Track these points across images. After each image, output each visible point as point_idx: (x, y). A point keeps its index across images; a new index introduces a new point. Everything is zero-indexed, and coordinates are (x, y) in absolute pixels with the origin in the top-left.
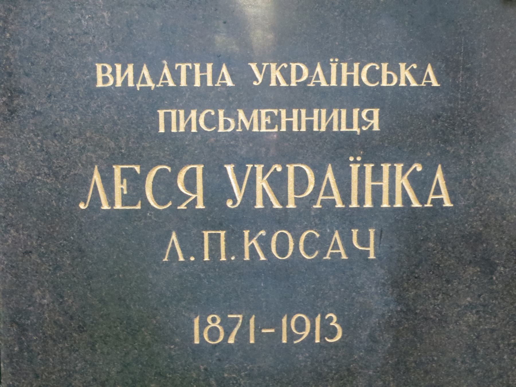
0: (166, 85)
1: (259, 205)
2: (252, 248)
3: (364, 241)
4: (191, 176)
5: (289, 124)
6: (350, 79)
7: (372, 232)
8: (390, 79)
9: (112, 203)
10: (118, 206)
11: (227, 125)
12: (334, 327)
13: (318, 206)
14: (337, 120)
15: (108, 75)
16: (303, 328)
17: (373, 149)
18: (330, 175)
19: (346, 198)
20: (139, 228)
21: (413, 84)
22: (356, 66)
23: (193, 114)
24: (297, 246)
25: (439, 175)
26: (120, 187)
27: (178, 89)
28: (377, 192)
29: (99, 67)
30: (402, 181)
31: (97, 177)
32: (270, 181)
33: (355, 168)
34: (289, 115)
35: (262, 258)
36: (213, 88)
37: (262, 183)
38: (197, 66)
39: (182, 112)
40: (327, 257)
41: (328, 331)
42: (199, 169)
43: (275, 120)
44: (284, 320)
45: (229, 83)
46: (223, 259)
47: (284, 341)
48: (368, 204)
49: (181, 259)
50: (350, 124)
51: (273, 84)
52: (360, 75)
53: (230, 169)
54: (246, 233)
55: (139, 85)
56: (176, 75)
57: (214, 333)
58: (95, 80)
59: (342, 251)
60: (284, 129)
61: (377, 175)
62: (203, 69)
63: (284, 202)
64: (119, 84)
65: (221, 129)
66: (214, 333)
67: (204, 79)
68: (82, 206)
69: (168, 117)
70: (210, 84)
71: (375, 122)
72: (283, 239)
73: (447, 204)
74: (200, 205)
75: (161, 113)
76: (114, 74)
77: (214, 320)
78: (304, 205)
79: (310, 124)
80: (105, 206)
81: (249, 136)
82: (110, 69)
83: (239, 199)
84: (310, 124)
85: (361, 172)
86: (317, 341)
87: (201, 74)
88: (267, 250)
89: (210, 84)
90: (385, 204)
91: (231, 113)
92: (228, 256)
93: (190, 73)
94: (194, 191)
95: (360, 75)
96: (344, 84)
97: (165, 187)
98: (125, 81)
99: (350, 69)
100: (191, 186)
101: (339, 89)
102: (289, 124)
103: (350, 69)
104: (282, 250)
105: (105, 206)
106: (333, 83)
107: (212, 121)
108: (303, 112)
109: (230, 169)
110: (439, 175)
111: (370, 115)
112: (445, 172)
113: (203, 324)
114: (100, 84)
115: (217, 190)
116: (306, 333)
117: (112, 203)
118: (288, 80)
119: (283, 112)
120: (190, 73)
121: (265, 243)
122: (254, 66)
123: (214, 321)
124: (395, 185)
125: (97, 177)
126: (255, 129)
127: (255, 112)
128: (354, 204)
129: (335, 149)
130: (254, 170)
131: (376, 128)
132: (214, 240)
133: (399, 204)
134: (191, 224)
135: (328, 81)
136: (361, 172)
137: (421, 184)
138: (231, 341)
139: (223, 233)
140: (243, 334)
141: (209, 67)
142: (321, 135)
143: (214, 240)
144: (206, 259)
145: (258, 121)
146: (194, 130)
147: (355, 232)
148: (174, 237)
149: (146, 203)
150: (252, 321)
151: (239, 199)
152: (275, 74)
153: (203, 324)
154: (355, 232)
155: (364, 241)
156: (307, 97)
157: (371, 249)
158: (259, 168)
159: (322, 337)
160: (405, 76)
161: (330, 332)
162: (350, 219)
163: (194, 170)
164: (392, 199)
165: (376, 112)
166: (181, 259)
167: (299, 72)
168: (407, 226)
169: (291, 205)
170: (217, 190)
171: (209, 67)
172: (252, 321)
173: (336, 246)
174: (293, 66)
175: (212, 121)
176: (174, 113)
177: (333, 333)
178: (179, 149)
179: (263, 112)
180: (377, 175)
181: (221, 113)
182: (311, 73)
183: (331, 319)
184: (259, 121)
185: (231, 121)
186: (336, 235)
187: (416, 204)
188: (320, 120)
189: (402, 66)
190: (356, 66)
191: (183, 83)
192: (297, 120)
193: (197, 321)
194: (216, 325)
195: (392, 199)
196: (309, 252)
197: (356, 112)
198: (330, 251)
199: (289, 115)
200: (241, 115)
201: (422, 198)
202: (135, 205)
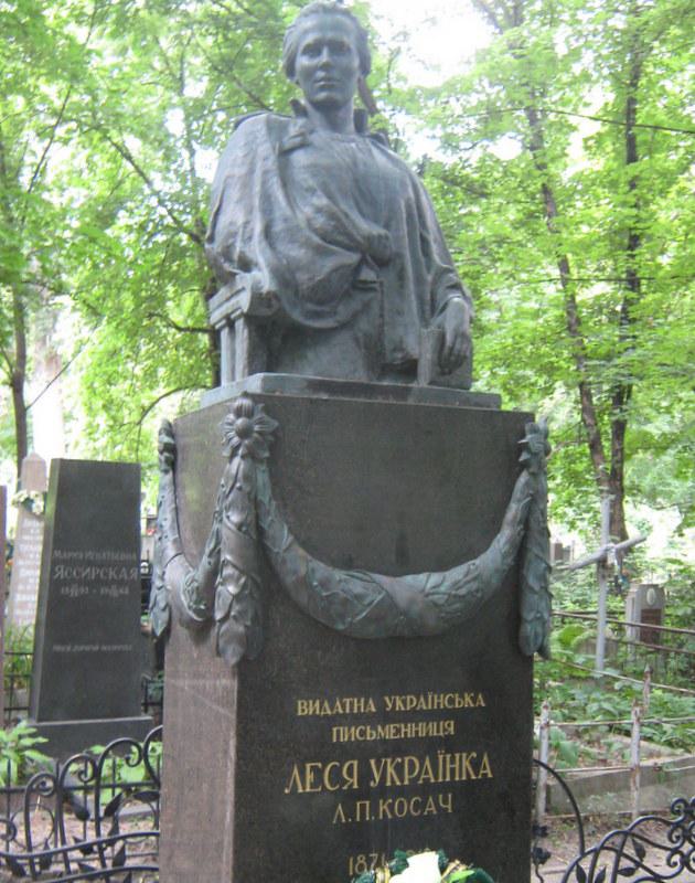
1: (389, 784)
2: (384, 811)
3: (445, 802)
4: (350, 769)
5: (406, 733)
6: (439, 704)
8: (459, 703)
9: (304, 788)
10: (308, 790)
13: (421, 782)
14: (432, 729)
15: (305, 707)
17: (450, 745)
18: (427, 763)
19: (436, 777)
21: (472, 705)
22: (442, 696)
23: (353, 729)
24: (409, 807)
25: (485, 759)
27: (344, 714)
28: (453, 770)
29: (300, 703)
30: (466, 763)
31: (296, 772)
32: (395, 768)
33: (441, 757)
34: (406, 727)
37: (390, 770)
38: (356, 701)
39: (346, 729)
40: (426, 813)
42: (355, 763)
43: (398, 731)
45: (373, 710)
46: (368, 819)
48: (448, 779)
49: (344, 821)
51: (397, 709)
52: (442, 701)
53: (373, 762)
55: (322, 713)
58: (296, 711)
59: (433, 808)
61: (453, 761)
62: (359, 702)
63: (402, 780)
64: (311, 713)
67: (359, 708)
68: (287, 791)
69: (338, 732)
70: (362, 710)
71: (452, 728)
73: (490, 776)
74: (356, 786)
75: (335, 729)
76: (308, 706)
79: (417, 732)
80: (300, 791)
81: (384, 741)
82: (305, 704)
83: (377, 780)
84: (417, 732)
87: (355, 705)
89: (362, 710)
90: (457, 779)
93: (352, 704)
95: (442, 701)
96: (435, 707)
97: (336, 776)
98: (315, 711)
99: (439, 698)
101: (432, 710)
102: (406, 733)
103: (439, 698)
104: (401, 811)
105: (300, 791)
106: (430, 707)
107: (363, 733)
109: (373, 762)
111: (449, 725)
112: (489, 756)
113: (355, 862)
114: (300, 713)
115: (365, 775)
117: (304, 788)
119: (403, 726)
120: (352, 704)
121: (391, 807)
122: (387, 699)
124: (459, 767)
128: (440, 780)
129: (428, 747)
130: (386, 763)
131: (452, 733)
132: (363, 807)
133: (464, 778)
134: (350, 798)
135: (427, 705)
137: (476, 765)
139: (367, 803)
141: (362, 700)
143: (363, 807)
145: (389, 732)
146: (353, 739)
147: (441, 796)
148: (340, 807)
149: (324, 787)
151: (377, 780)
152: (399, 703)
153: (355, 862)
154: (441, 796)
155: (445, 802)
156: (413, 716)
157: (449, 806)
158: (389, 761)
160: (468, 701)
164: (461, 776)
165: (452, 723)
166: (344, 821)
167: (412, 701)
168: (465, 791)
169: (406, 782)
170: (365, 775)
171: (362, 700)
174: (409, 698)
176: (341, 729)
178: (345, 751)
180: (453, 761)
181: (368, 728)
184: (389, 732)
185: (374, 733)
186: (431, 799)
187: (473, 777)
188: (422, 729)
189: (466, 695)
190: (442, 696)
191: (348, 711)
192: (409, 730)
193: (351, 860)
194: (362, 862)
195: (461, 776)
196: (416, 811)
197: (441, 723)
198: (427, 809)
199: (406, 727)
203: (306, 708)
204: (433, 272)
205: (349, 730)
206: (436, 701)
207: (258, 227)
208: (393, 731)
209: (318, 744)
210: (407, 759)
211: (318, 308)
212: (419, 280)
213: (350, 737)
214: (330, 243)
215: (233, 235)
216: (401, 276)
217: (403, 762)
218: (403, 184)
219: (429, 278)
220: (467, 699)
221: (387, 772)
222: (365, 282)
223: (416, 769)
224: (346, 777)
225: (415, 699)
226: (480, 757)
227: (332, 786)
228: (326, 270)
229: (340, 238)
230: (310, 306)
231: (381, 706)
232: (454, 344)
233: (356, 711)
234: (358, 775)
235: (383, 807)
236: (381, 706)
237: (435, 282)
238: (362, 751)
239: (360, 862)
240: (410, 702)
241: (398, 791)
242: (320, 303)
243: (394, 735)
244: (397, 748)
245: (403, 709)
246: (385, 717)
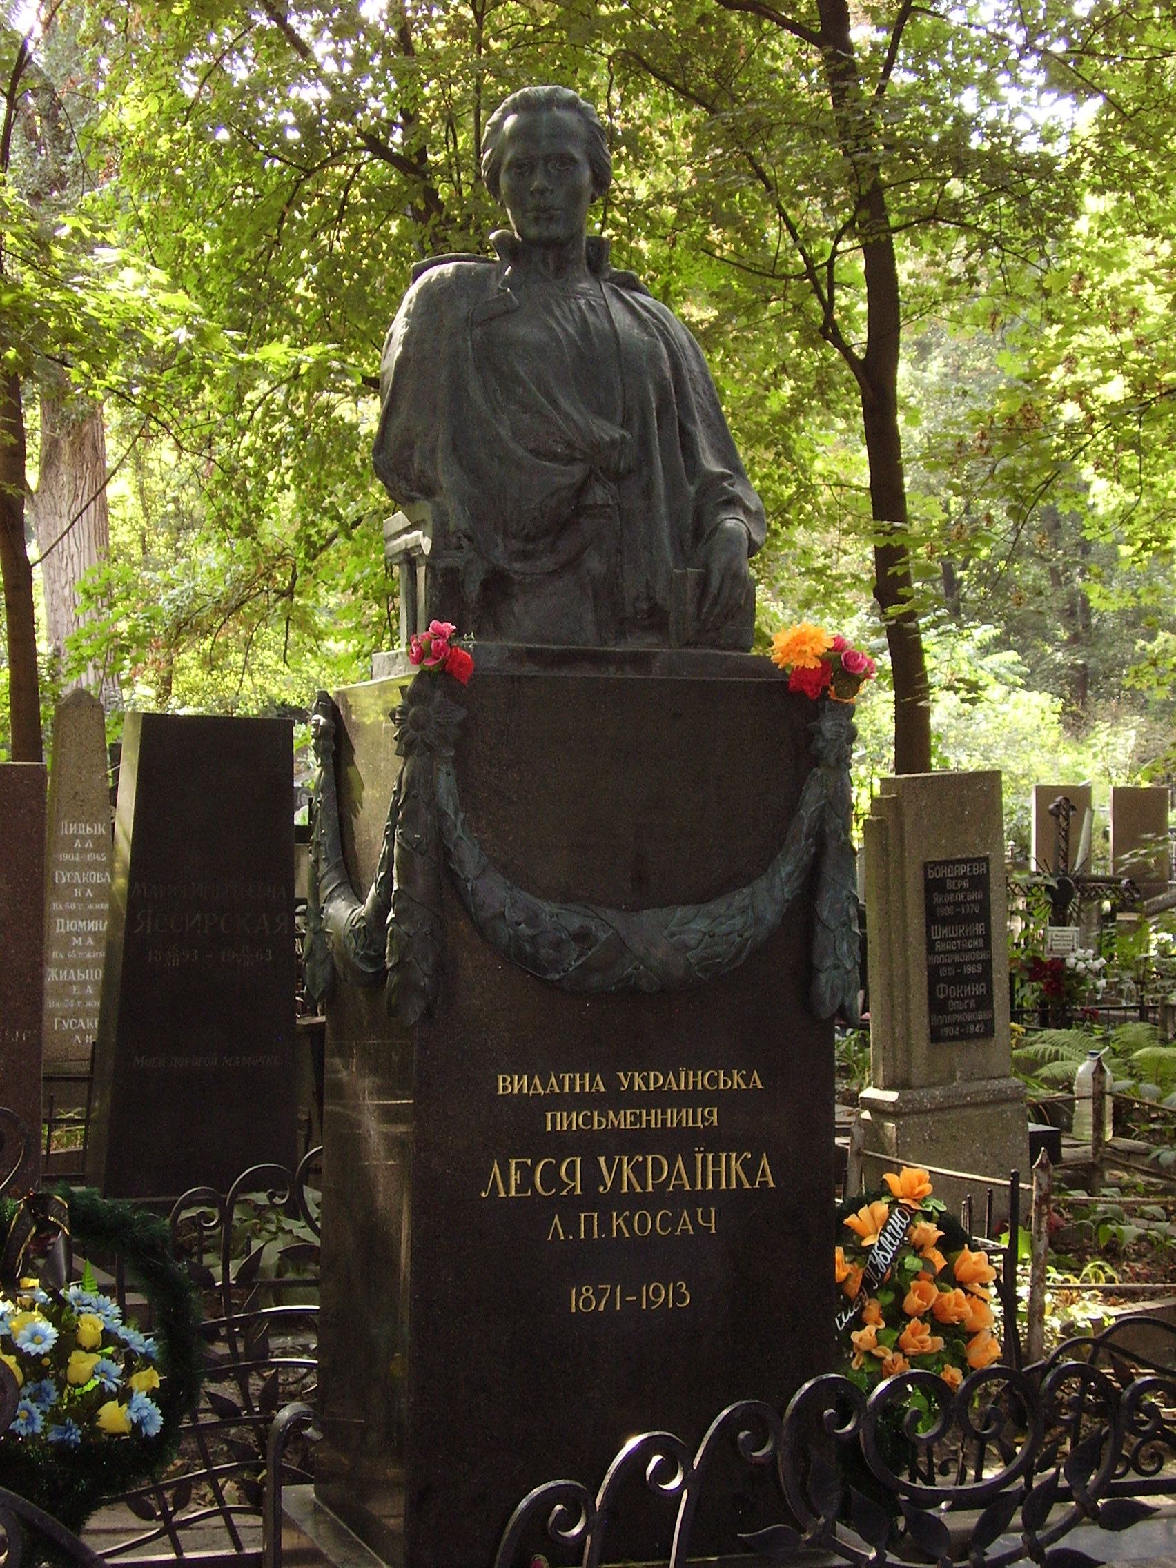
1: (625, 1190)
3: (707, 1218)
4: (572, 1165)
5: (648, 1122)
6: (695, 1083)
8: (725, 1083)
9: (507, 1191)
11: (600, 1123)
14: (685, 1118)
16: (659, 1295)
17: (713, 1140)
18: (680, 1163)
19: (693, 1183)
20: (531, 1211)
24: (654, 1223)
25: (765, 1161)
26: (514, 1177)
28: (716, 1176)
31: (496, 1170)
33: (699, 1156)
41: (679, 1297)
43: (638, 1118)
50: (695, 1121)
52: (703, 1080)
53: (602, 1160)
56: (561, 1083)
57: (587, 1302)
58: (497, 1089)
61: (716, 1163)
62: (582, 1078)
63: (644, 1187)
67: (582, 1086)
69: (554, 1117)
75: (549, 1115)
76: (512, 1083)
79: (664, 1121)
80: (503, 1195)
81: (616, 1131)
84: (664, 1121)
85: (704, 1159)
87: (580, 1082)
90: (724, 1186)
91: (603, 1114)
93: (572, 1081)
94: (573, 1179)
98: (521, 1089)
99: (695, 1076)
102: (648, 1122)
103: (695, 1076)
104: (643, 1227)
107: (588, 1120)
109: (602, 1160)
110: (765, 1161)
111: (710, 1113)
113: (579, 1294)
115: (592, 1177)
118: (647, 1086)
120: (572, 1081)
121: (629, 1222)
122: (621, 1074)
123: (587, 1291)
124: (729, 1170)
125: (496, 1170)
129: (677, 1143)
132: (589, 1220)
133: (734, 1186)
134: (570, 1207)
136: (704, 1159)
137: (750, 1168)
138: (602, 1308)
140: (611, 1302)
143: (589, 1220)
145: (624, 1120)
148: (556, 1219)
152: (638, 1080)
155: (707, 1218)
156: (661, 1099)
163: (573, 1162)
170: (592, 1177)
173: (685, 1224)
178: (562, 1144)
180: (716, 1163)
182: (665, 1080)
184: (624, 1120)
187: (747, 1186)
188: (672, 1117)
191: (567, 1089)
192: (653, 1118)
201: (752, 1181)
203: (511, 1085)
206: (691, 1080)
207: (443, 439)
209: (523, 1131)
213: (570, 1125)
215: (410, 446)
216: (648, 492)
217: (645, 1160)
218: (654, 357)
220: (736, 1077)
223: (664, 1171)
226: (756, 1160)
231: (613, 1083)
232: (720, 589)
236: (613, 1083)
237: (701, 493)
238: (588, 1145)
240: (656, 1080)
241: (636, 1201)
244: (635, 1142)
246: (615, 1099)
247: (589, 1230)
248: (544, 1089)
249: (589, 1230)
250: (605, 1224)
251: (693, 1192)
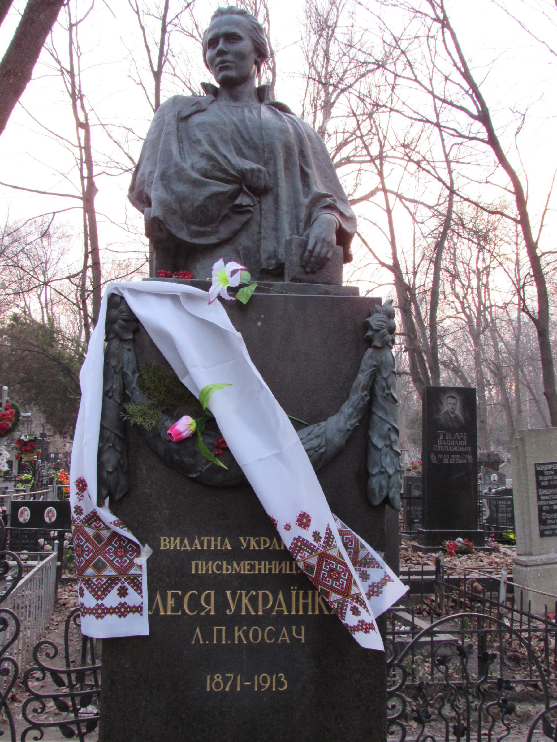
0: (196, 548)
1: (244, 613)
3: (299, 633)
5: (260, 570)
7: (303, 628)
9: (166, 611)
10: (169, 613)
11: (227, 569)
12: (283, 682)
13: (274, 613)
15: (167, 543)
16: (267, 682)
18: (281, 596)
19: (289, 609)
23: (210, 563)
27: (202, 551)
29: (162, 538)
32: (249, 600)
33: (294, 593)
35: (245, 642)
36: (221, 550)
37: (245, 601)
38: (213, 539)
39: (204, 563)
40: (279, 642)
42: (212, 593)
43: (252, 567)
44: (256, 677)
45: (229, 548)
47: (256, 690)
48: (301, 612)
51: (252, 548)
53: (228, 593)
54: (236, 628)
55: (182, 549)
56: (202, 544)
58: (159, 545)
59: (287, 638)
60: (257, 572)
62: (216, 540)
63: (256, 611)
65: (224, 572)
66: (218, 685)
67: (216, 545)
69: (197, 565)
72: (256, 631)
74: (212, 613)
75: (194, 563)
76: (170, 542)
77: (218, 677)
78: (267, 612)
79: (270, 569)
80: (162, 613)
81: (238, 575)
82: (168, 540)
83: (233, 609)
84: (270, 569)
86: (274, 689)
87: (214, 543)
88: (247, 638)
89: (219, 548)
91: (230, 563)
92: (226, 641)
93: (209, 542)
94: (209, 605)
97: (194, 603)
100: (208, 602)
102: (260, 570)
104: (255, 637)
105: (162, 613)
107: (219, 567)
108: (267, 563)
109: (228, 593)
113: (212, 679)
115: (222, 604)
116: (267, 685)
117: (166, 611)
118: (259, 547)
119: (257, 563)
120: (209, 542)
121: (246, 634)
122: (242, 539)
123: (218, 678)
126: (242, 572)
127: (242, 563)
128: (294, 613)
130: (241, 594)
132: (219, 632)
133: (317, 612)
134: (207, 623)
138: (227, 689)
139: (224, 628)
140: (234, 685)
141: (219, 539)
142: (275, 575)
143: (219, 632)
144: (215, 642)
145: (244, 568)
147: (294, 628)
148: (198, 630)
150: (239, 677)
151: (233, 609)
152: (253, 543)
153: (212, 679)
154: (294, 628)
155: (299, 633)
157: (303, 637)
158: (244, 593)
159: (276, 688)
161: (281, 684)
162: (290, 621)
163: (209, 594)
164: (313, 610)
169: (260, 613)
170: (222, 604)
172: (239, 677)
173: (284, 636)
174: (262, 539)
175: (219, 567)
176: (200, 563)
177: (282, 685)
179: (246, 563)
180: (305, 597)
181: (225, 563)
182: (271, 542)
183: (281, 676)
184: (244, 568)
185: (229, 567)
186: (284, 630)
191: (205, 548)
193: (209, 677)
194: (219, 680)
195: (313, 610)
196: (270, 639)
198: (281, 638)
200: (235, 565)
202: (178, 612)
204: (310, 197)
205: (207, 564)
208: (247, 567)
210: (260, 593)
211: (202, 229)
212: (296, 205)
213: (207, 570)
214: (208, 178)
216: (276, 201)
217: (257, 594)
219: (305, 201)
221: (242, 602)
222: (240, 206)
224: (204, 605)
225: (267, 539)
227: (191, 611)
228: (201, 198)
229: (219, 174)
230: (194, 228)
231: (236, 544)
232: (314, 248)
233: (213, 548)
234: (215, 604)
235: (238, 633)
236: (236, 544)
238: (218, 583)
239: (217, 680)
242: (201, 224)
243: (249, 570)
245: (257, 548)
246: (237, 554)
247: (219, 638)
248: (191, 546)
249: (219, 638)
250: (230, 634)
251: (290, 616)
